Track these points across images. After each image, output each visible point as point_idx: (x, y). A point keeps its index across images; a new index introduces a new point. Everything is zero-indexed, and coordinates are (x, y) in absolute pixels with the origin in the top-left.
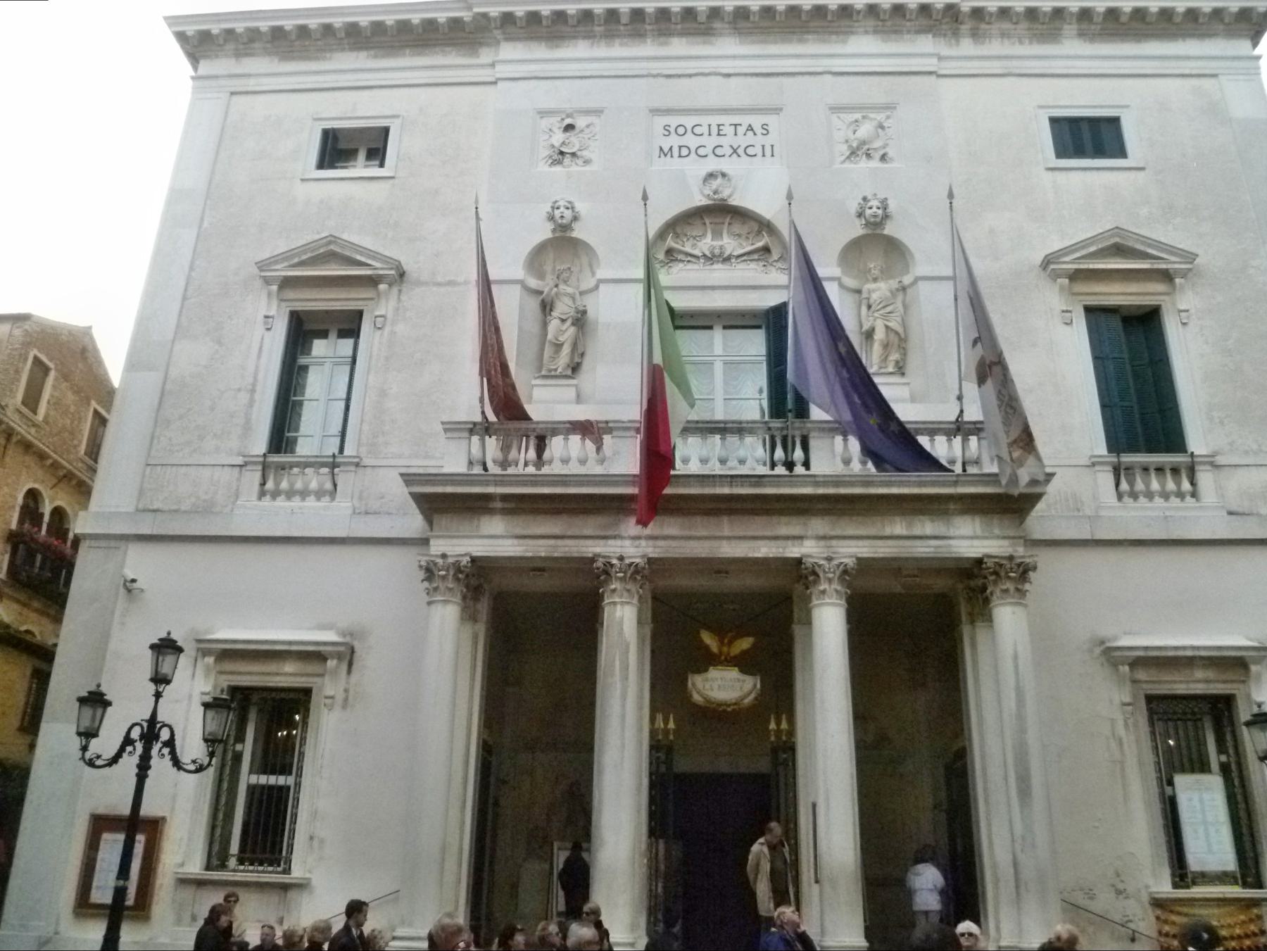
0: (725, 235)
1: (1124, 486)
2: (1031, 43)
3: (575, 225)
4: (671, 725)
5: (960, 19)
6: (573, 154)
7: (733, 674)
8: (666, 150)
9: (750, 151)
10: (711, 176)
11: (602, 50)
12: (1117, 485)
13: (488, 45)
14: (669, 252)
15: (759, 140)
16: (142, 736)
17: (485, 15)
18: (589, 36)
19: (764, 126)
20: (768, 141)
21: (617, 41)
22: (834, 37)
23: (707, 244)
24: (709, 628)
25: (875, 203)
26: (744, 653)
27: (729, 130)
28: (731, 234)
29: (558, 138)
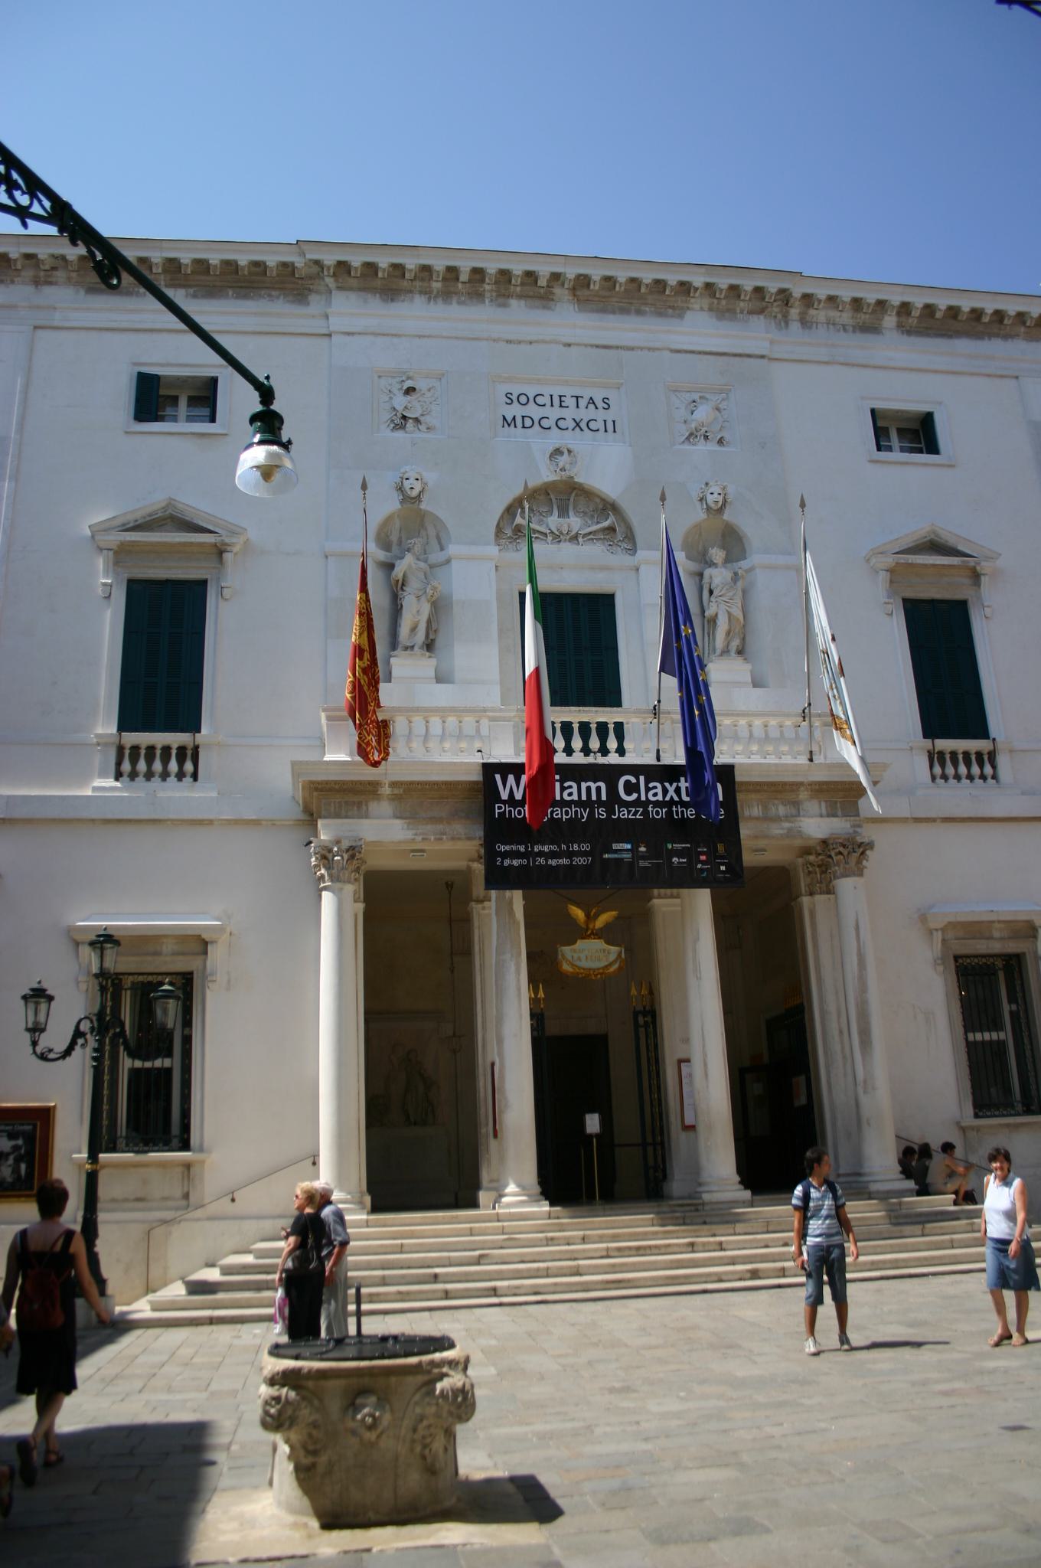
0: (571, 513)
1: (938, 770)
2: (854, 331)
3: (425, 498)
4: (541, 995)
5: (792, 301)
6: (417, 420)
7: (598, 944)
8: (509, 420)
9: (592, 425)
10: (558, 452)
11: (438, 309)
12: (931, 767)
13: (317, 292)
14: (518, 529)
15: (601, 415)
16: (92, 1029)
17: (317, 262)
18: (427, 292)
19: (605, 400)
20: (609, 416)
21: (455, 299)
22: (670, 311)
23: (554, 521)
24: (578, 905)
25: (716, 489)
26: (608, 926)
27: (570, 402)
28: (577, 512)
29: (400, 401)
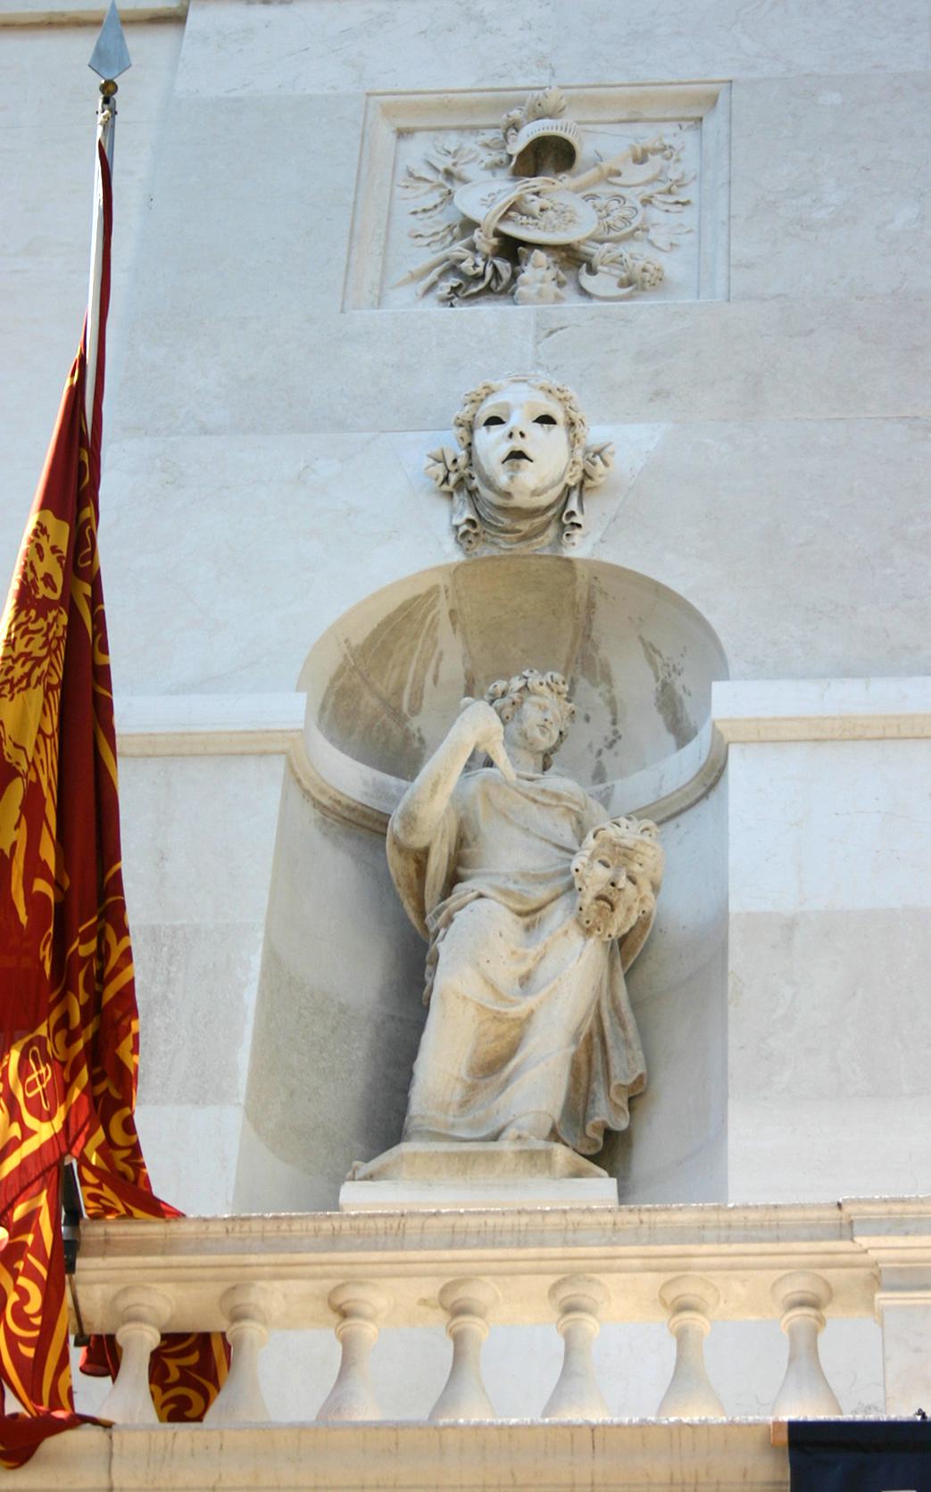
3: (592, 515)
